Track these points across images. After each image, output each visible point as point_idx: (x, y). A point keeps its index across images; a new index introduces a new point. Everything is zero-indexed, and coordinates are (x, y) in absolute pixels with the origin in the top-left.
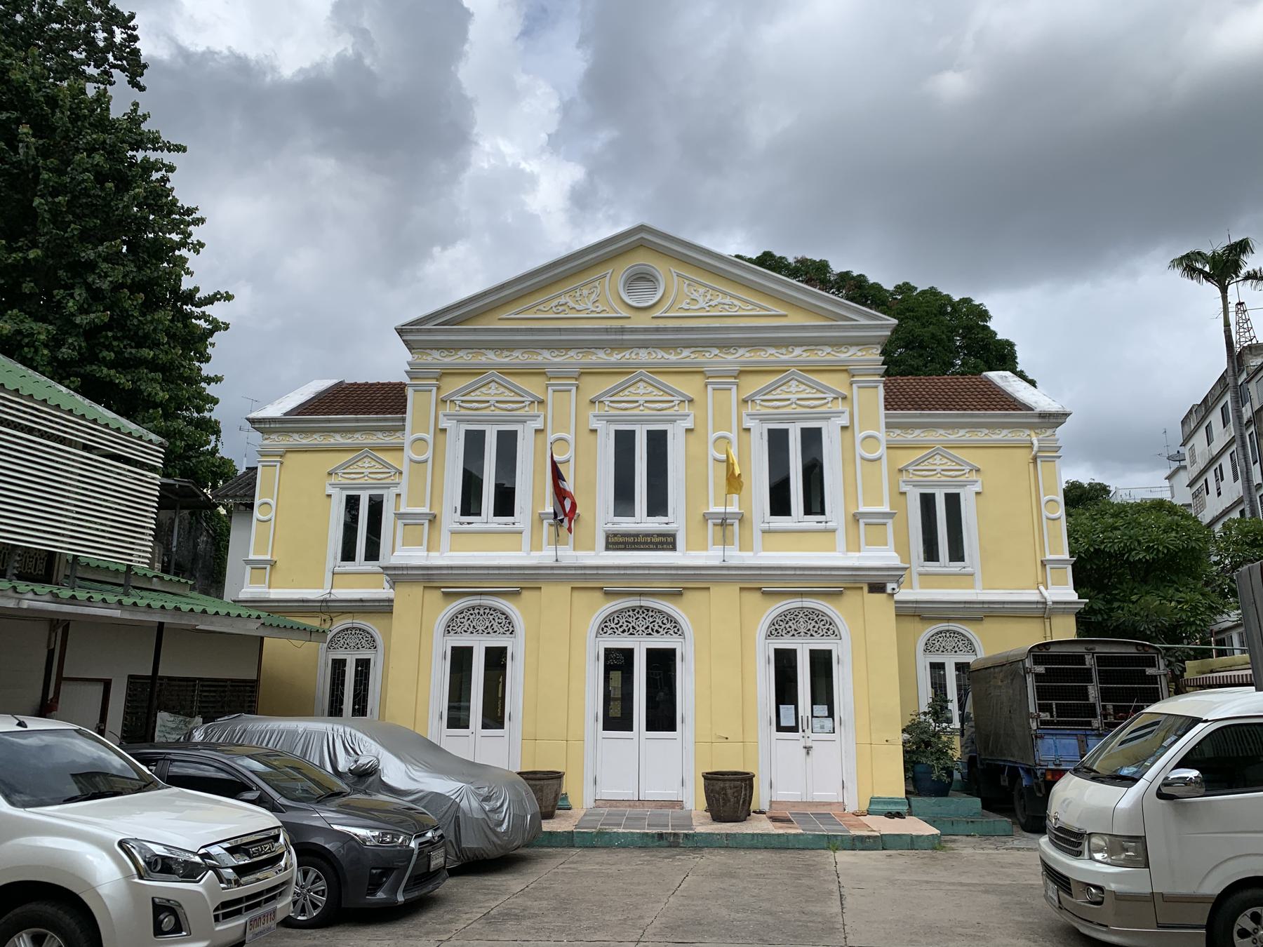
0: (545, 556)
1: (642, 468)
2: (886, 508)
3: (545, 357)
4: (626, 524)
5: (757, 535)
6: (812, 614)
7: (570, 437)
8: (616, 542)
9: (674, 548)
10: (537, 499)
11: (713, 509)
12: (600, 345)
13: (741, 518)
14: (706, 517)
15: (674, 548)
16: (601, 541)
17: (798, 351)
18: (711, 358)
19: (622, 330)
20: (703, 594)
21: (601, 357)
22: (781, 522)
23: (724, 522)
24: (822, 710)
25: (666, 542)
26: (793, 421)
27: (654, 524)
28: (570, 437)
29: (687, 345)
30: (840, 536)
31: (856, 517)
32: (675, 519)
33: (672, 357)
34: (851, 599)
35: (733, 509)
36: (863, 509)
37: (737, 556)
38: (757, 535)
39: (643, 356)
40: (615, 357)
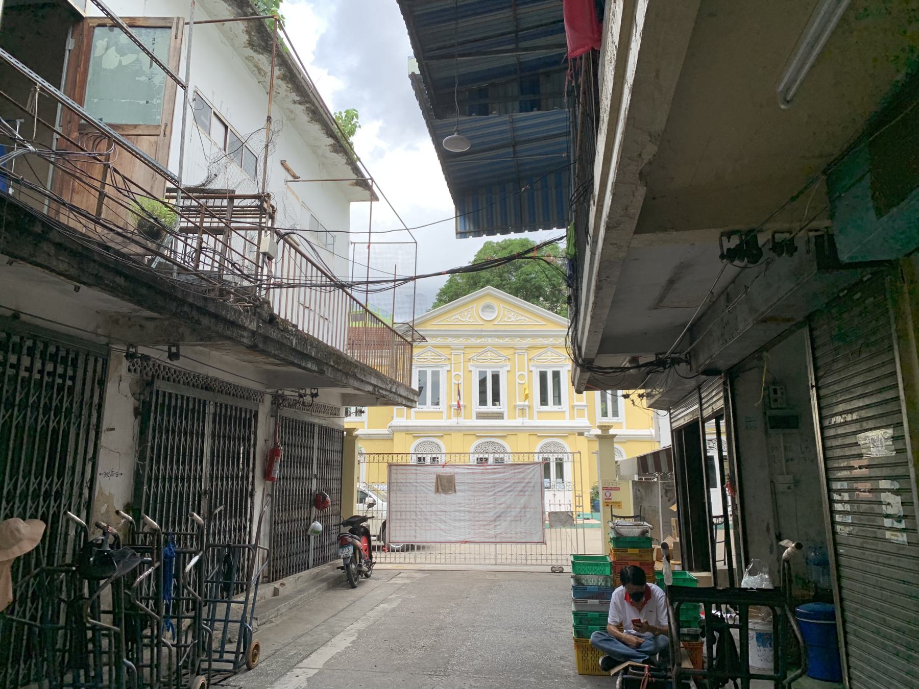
0: (453, 422)
1: (490, 389)
2: (584, 403)
3: (450, 341)
4: (484, 409)
5: (535, 414)
6: (555, 444)
7: (461, 374)
8: (481, 416)
9: (503, 418)
10: (449, 399)
11: (518, 403)
12: (472, 336)
13: (529, 407)
14: (515, 407)
15: (503, 418)
16: (474, 416)
17: (551, 339)
18: (517, 342)
19: (482, 331)
20: (514, 437)
21: (473, 341)
22: (544, 408)
23: (523, 409)
24: (560, 480)
25: (500, 416)
26: (549, 367)
27: (495, 409)
28: (461, 374)
29: (507, 336)
30: (567, 414)
31: (573, 407)
32: (503, 406)
33: (501, 341)
34: (571, 438)
35: (526, 403)
36: (576, 403)
37: (528, 422)
38: (535, 414)
39: (490, 340)
40: (479, 341)
